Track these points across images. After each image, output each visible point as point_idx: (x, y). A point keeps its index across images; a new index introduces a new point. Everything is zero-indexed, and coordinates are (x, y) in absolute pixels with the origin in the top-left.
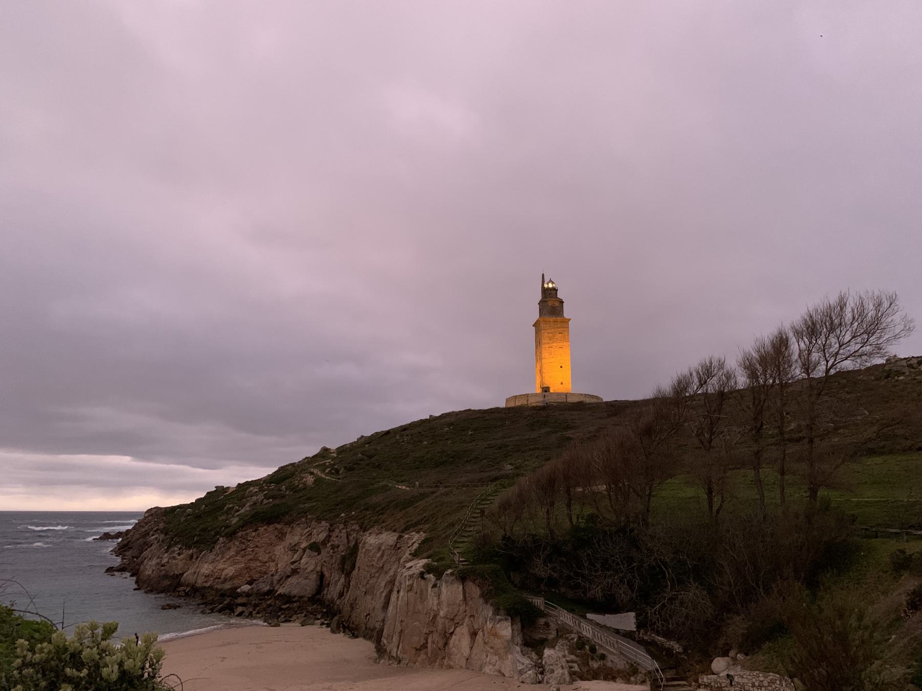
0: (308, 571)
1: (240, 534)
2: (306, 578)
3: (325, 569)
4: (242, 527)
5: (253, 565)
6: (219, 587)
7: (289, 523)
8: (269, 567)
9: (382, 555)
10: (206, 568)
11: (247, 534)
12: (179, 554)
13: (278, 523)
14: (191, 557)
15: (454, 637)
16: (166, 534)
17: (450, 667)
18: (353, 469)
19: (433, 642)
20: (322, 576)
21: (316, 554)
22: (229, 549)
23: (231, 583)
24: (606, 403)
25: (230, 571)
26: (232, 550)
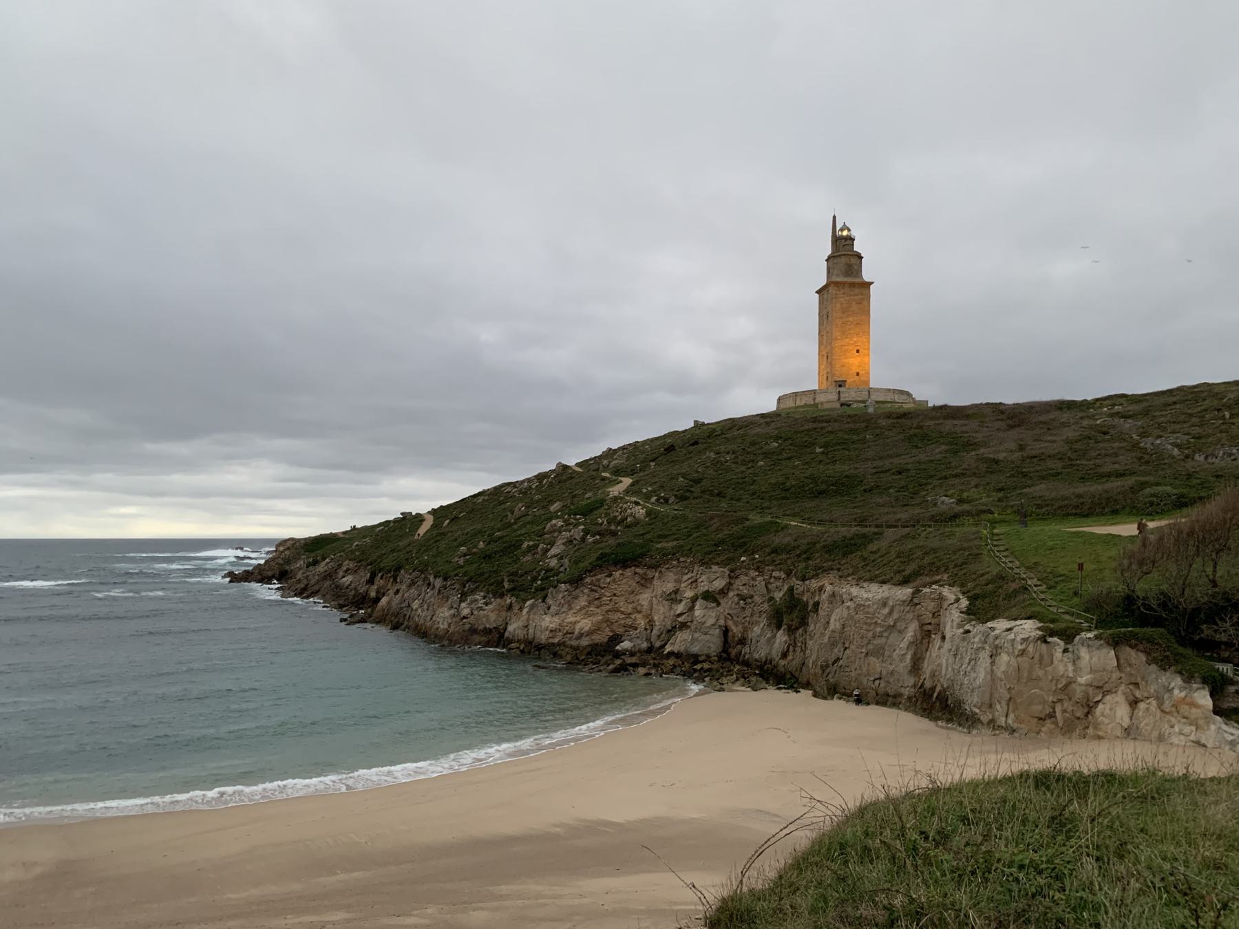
0: (708, 624)
1: (588, 580)
3: (730, 623)
5: (613, 617)
6: (574, 643)
7: (655, 567)
8: (635, 620)
9: (891, 613)
10: (549, 622)
11: (598, 580)
12: (487, 604)
14: (510, 607)
15: (1101, 706)
16: (445, 579)
17: (1099, 738)
18: (686, 498)
19: (1065, 711)
20: (726, 631)
22: (576, 598)
24: (935, 408)
25: (585, 624)
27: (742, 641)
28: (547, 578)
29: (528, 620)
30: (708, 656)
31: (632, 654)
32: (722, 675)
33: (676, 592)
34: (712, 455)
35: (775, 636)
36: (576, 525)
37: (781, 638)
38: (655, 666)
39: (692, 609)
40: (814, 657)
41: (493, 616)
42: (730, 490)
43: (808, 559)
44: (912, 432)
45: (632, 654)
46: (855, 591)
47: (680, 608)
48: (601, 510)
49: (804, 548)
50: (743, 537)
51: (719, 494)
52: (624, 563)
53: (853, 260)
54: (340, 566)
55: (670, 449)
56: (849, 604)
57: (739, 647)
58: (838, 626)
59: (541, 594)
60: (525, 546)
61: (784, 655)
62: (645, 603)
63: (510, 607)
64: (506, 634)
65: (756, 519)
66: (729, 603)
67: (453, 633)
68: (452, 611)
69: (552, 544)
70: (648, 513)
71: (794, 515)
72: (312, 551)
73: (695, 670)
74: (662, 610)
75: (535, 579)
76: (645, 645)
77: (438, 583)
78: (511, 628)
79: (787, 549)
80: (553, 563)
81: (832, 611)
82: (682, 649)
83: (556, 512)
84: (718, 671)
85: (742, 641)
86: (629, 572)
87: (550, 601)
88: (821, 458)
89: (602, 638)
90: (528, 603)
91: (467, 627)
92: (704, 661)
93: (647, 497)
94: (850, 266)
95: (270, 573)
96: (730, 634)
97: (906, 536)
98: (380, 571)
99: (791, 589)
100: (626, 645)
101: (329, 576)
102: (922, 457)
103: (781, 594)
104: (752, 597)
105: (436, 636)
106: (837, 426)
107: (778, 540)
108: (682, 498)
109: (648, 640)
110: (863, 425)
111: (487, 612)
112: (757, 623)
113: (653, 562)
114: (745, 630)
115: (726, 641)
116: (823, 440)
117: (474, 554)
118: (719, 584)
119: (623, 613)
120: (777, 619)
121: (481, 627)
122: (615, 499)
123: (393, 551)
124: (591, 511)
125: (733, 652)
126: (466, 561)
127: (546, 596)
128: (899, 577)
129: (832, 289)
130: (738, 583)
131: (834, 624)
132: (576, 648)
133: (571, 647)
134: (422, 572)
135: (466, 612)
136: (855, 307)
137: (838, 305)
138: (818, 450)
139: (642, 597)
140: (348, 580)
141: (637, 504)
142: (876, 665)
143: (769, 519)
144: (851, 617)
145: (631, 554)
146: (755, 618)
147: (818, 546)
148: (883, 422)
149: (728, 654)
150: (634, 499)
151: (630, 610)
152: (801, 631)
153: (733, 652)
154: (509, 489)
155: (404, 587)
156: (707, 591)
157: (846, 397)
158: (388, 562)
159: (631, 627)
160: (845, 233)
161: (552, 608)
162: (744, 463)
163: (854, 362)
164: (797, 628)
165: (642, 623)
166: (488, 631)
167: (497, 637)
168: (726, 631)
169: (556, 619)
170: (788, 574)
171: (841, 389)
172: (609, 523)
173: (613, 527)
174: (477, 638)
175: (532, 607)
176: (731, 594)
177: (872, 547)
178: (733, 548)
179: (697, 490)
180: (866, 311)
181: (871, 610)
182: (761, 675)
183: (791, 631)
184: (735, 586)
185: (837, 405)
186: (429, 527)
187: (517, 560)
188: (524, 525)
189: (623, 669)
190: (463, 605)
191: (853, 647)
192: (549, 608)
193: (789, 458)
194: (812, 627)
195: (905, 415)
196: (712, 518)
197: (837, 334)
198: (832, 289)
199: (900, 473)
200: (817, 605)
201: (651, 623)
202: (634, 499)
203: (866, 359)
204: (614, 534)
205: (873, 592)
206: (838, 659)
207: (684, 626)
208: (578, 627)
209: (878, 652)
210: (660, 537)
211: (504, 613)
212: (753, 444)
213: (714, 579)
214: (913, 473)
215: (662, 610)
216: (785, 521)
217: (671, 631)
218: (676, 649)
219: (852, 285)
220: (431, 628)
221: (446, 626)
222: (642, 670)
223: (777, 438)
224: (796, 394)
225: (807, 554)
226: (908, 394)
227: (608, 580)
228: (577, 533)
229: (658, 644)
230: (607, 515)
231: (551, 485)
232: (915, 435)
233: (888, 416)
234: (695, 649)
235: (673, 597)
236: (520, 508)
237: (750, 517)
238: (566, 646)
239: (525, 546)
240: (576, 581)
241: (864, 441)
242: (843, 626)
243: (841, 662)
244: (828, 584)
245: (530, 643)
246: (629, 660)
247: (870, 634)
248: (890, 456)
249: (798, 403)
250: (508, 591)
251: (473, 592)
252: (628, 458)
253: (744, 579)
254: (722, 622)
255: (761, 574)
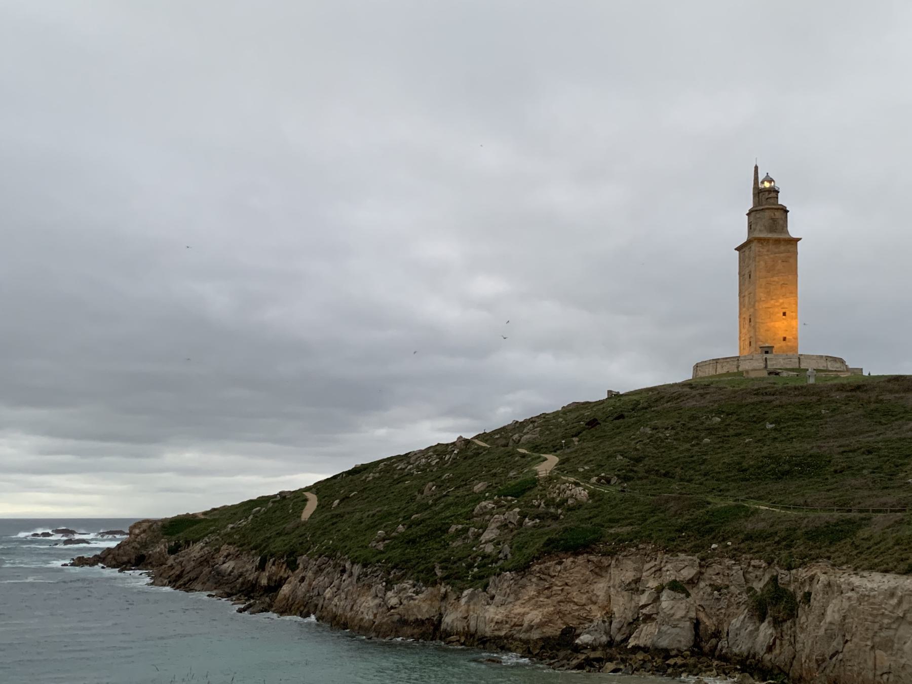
1: (536, 568)
2: (675, 626)
3: (702, 616)
4: (538, 559)
6: (523, 636)
7: (611, 554)
9: (900, 602)
10: (493, 613)
11: (548, 568)
12: (417, 593)
13: (591, 553)
14: (445, 597)
16: (365, 566)
20: (697, 624)
21: (683, 595)
23: (539, 631)
25: (534, 616)
26: (529, 588)
27: (717, 634)
28: (485, 565)
29: (467, 611)
30: (678, 650)
31: (594, 649)
32: (700, 671)
33: (637, 581)
34: (649, 431)
35: (757, 629)
36: (510, 507)
37: (766, 631)
38: (623, 661)
39: (657, 599)
40: (807, 651)
41: (425, 607)
42: (678, 469)
43: (789, 546)
44: (873, 406)
45: (594, 649)
46: (856, 580)
47: (644, 599)
48: (535, 491)
49: (783, 534)
50: (708, 522)
51: (666, 475)
52: (576, 550)
53: (778, 214)
54: (218, 550)
55: (593, 423)
56: (850, 594)
57: (714, 641)
58: (837, 616)
59: (481, 581)
60: (453, 529)
61: (770, 649)
62: (601, 594)
63: (445, 597)
64: (443, 626)
65: (719, 503)
66: (699, 594)
67: (381, 624)
68: (377, 601)
69: (484, 528)
70: (592, 495)
71: (760, 498)
72: (172, 534)
73: (669, 666)
74: (621, 601)
75: (470, 566)
76: (604, 639)
77: (357, 569)
78: (448, 619)
79: (761, 536)
80: (489, 549)
81: (828, 602)
82: (649, 643)
83: (482, 492)
84: (695, 666)
85: (717, 634)
86: (581, 559)
87: (492, 590)
88: (773, 434)
89: (553, 631)
90: (466, 592)
91: (396, 617)
92: (676, 656)
93: (586, 477)
94: (774, 220)
95: (125, 559)
96: (702, 627)
97: (900, 522)
98: (272, 556)
99: (774, 579)
100: (585, 638)
101: (204, 561)
102: (889, 434)
103: (761, 585)
104: (727, 587)
105: (360, 627)
106: (785, 399)
107: (749, 526)
108: (626, 479)
109: (607, 633)
110: (814, 398)
111: (421, 604)
112: (735, 615)
113: (609, 548)
114: (720, 622)
115: (697, 635)
116: (772, 415)
117: (395, 538)
118: (688, 573)
119: (576, 604)
120: (760, 610)
121: (412, 618)
122: (550, 479)
123: (279, 534)
124: (523, 492)
125: (707, 647)
126: (386, 546)
127: (487, 585)
128: (903, 566)
129: (755, 246)
130: (709, 572)
131: (832, 614)
132: (526, 642)
133: (521, 640)
134: (330, 557)
135: (394, 601)
136: (780, 266)
137: (762, 263)
138: (769, 426)
139: (595, 586)
140: (229, 566)
141: (577, 484)
142: (884, 659)
143: (731, 502)
144: (852, 608)
145: (580, 541)
146: (732, 610)
147: (799, 532)
148: (837, 396)
149: (701, 648)
150: (572, 479)
151: (584, 601)
152: (789, 623)
153: (707, 647)
154: (401, 466)
155: (310, 574)
156: (675, 581)
157: (773, 365)
158: (278, 545)
159: (585, 618)
160: (767, 185)
161: (497, 598)
162: (687, 440)
163: (780, 326)
164: (785, 621)
165: (598, 614)
166: (419, 623)
167: (431, 631)
168: (697, 624)
169: (501, 610)
170: (769, 564)
171: (768, 356)
172: (547, 505)
173: (552, 510)
174: (408, 630)
175: (471, 597)
176: (702, 584)
177: (864, 533)
178: (700, 533)
179: (640, 468)
180: (793, 270)
181: (877, 600)
182: (743, 671)
183: (777, 623)
184: (706, 575)
185: (765, 374)
186: (315, 507)
187: (446, 546)
188: (447, 507)
189: (587, 664)
190: (390, 594)
191: (855, 640)
192: (493, 598)
193: (737, 435)
194: (803, 619)
195: (858, 388)
196: (667, 501)
197: (761, 295)
198: (755, 246)
199: (870, 452)
200: (807, 596)
201: (610, 615)
202: (572, 479)
203: (793, 323)
204: (556, 518)
205: (877, 582)
206: (837, 653)
207: (648, 618)
208: (527, 619)
209: (887, 645)
210: (610, 521)
211: (437, 604)
212: (693, 418)
213: (682, 567)
214: (884, 452)
215: (621, 601)
216: (752, 505)
217: (634, 624)
218: (641, 643)
219: (777, 241)
220: (352, 619)
221: (371, 617)
222: (610, 666)
223: (719, 413)
224: (717, 361)
225: (788, 540)
226: (842, 361)
227: (559, 568)
228: (513, 515)
229: (618, 638)
230: (543, 496)
231: (455, 462)
232: (877, 410)
233: (841, 388)
234: (664, 643)
235: (634, 586)
236: (430, 488)
237: (709, 499)
238: (515, 640)
239: (453, 529)
240: (523, 569)
241: (819, 416)
242: (844, 618)
243: (840, 656)
244: (821, 573)
245: (472, 635)
246: (593, 655)
247: (876, 626)
248: (854, 434)
249: (720, 371)
250: (443, 579)
251: (399, 579)
252: (541, 433)
253: (717, 568)
254: (693, 614)
255: (738, 561)
